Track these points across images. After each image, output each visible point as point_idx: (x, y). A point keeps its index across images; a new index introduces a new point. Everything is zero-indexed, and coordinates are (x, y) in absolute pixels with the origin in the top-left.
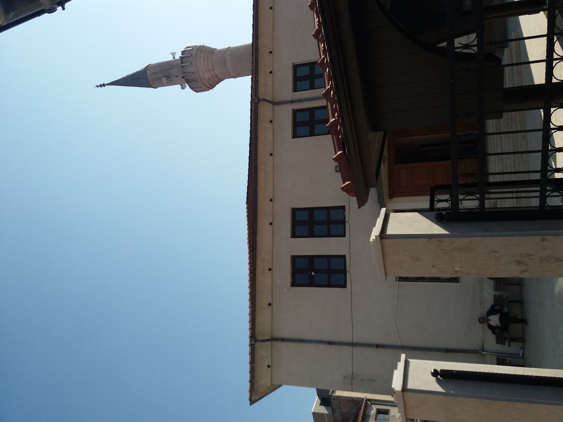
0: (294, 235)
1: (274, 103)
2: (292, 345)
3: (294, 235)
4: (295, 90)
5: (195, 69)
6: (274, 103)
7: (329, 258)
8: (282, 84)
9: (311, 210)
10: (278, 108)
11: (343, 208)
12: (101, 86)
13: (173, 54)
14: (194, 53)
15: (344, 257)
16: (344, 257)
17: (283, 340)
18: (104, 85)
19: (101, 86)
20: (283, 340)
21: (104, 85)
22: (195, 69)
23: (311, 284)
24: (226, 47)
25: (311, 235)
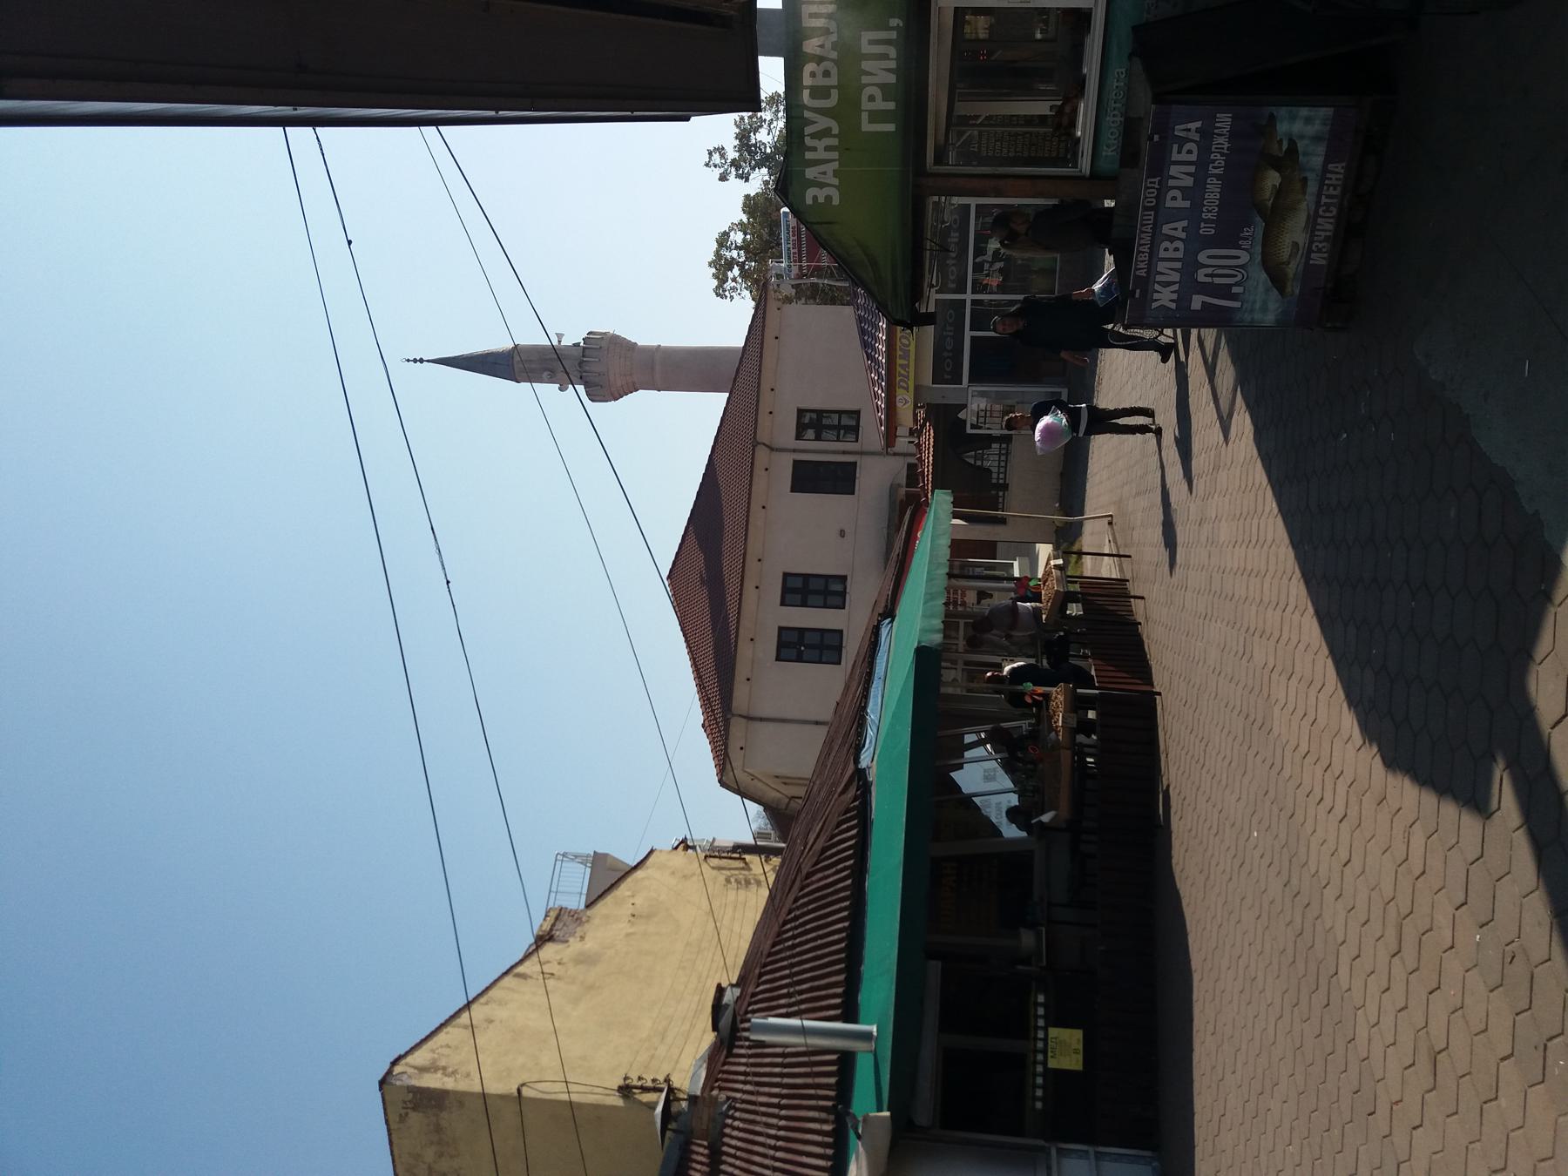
0: (783, 604)
1: (772, 449)
2: (771, 726)
3: (783, 604)
4: (799, 437)
5: (601, 368)
6: (772, 449)
7: (822, 631)
8: (780, 426)
9: (806, 577)
10: (776, 455)
11: (843, 579)
12: (415, 361)
13: (560, 336)
14: (604, 344)
15: (841, 632)
16: (841, 632)
17: (761, 719)
18: (421, 361)
19: (415, 361)
20: (761, 719)
21: (421, 361)
22: (601, 368)
23: (799, 659)
24: (655, 344)
25: (804, 604)
